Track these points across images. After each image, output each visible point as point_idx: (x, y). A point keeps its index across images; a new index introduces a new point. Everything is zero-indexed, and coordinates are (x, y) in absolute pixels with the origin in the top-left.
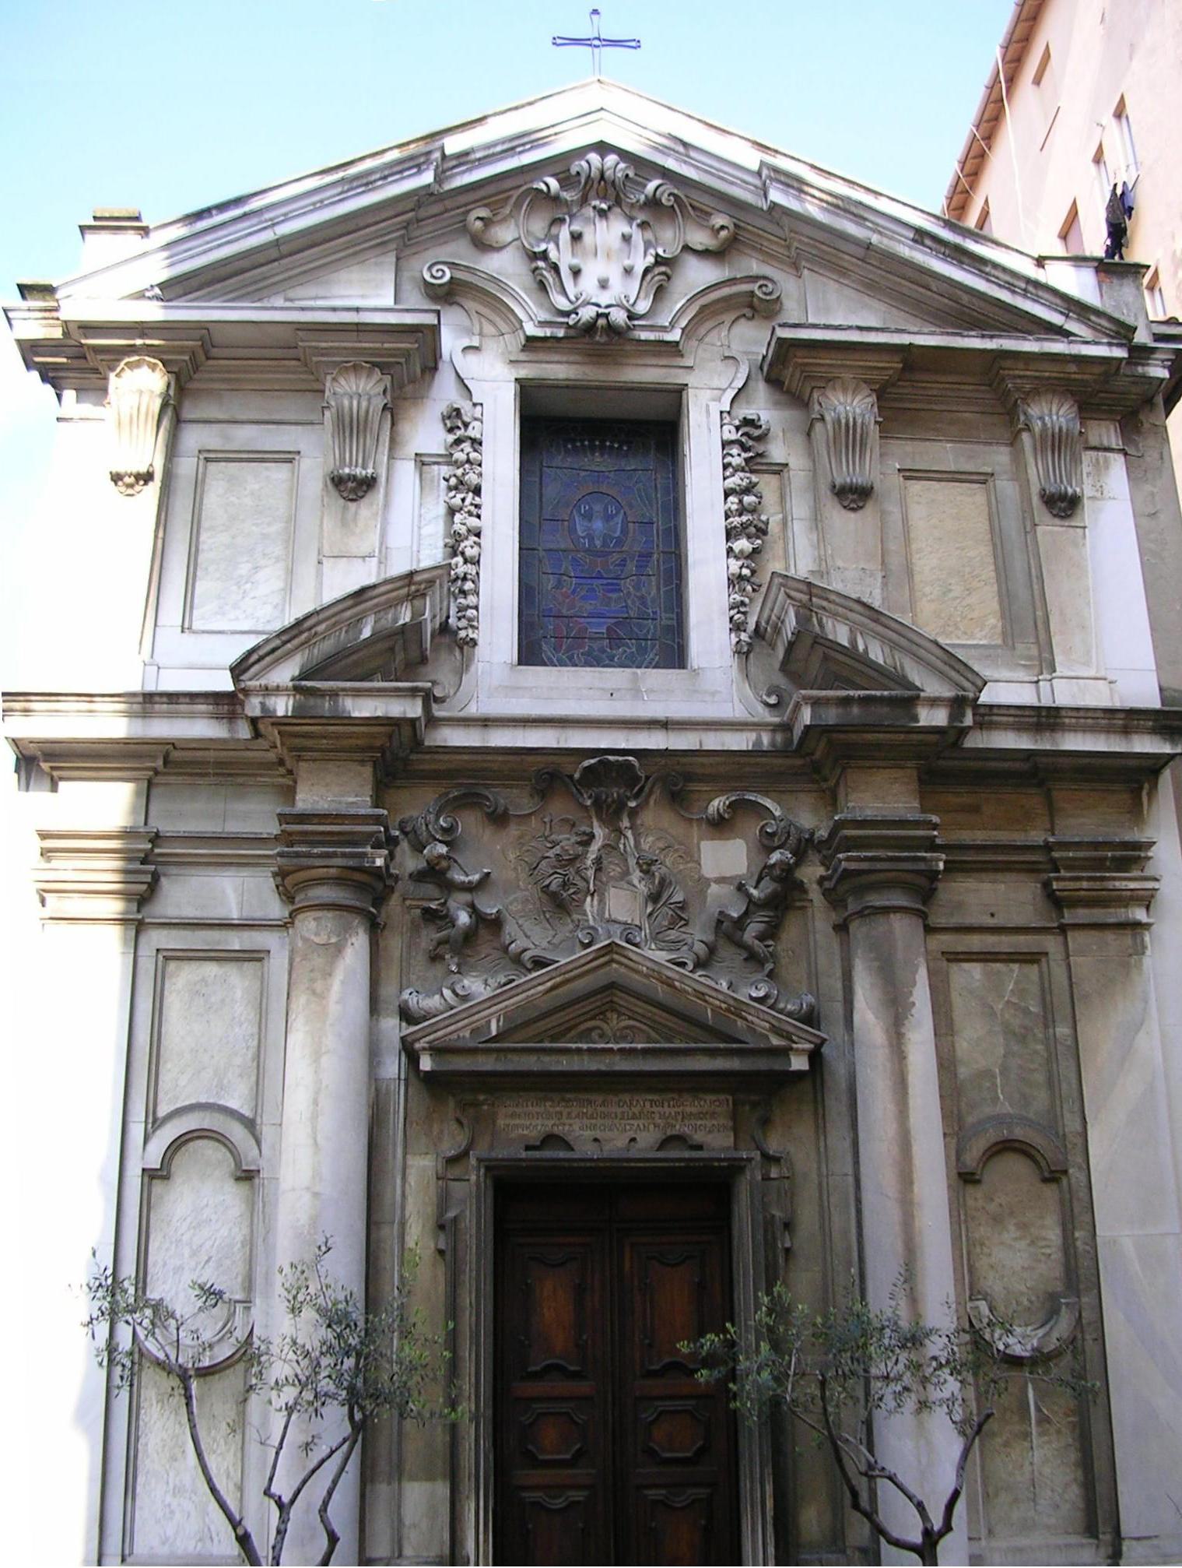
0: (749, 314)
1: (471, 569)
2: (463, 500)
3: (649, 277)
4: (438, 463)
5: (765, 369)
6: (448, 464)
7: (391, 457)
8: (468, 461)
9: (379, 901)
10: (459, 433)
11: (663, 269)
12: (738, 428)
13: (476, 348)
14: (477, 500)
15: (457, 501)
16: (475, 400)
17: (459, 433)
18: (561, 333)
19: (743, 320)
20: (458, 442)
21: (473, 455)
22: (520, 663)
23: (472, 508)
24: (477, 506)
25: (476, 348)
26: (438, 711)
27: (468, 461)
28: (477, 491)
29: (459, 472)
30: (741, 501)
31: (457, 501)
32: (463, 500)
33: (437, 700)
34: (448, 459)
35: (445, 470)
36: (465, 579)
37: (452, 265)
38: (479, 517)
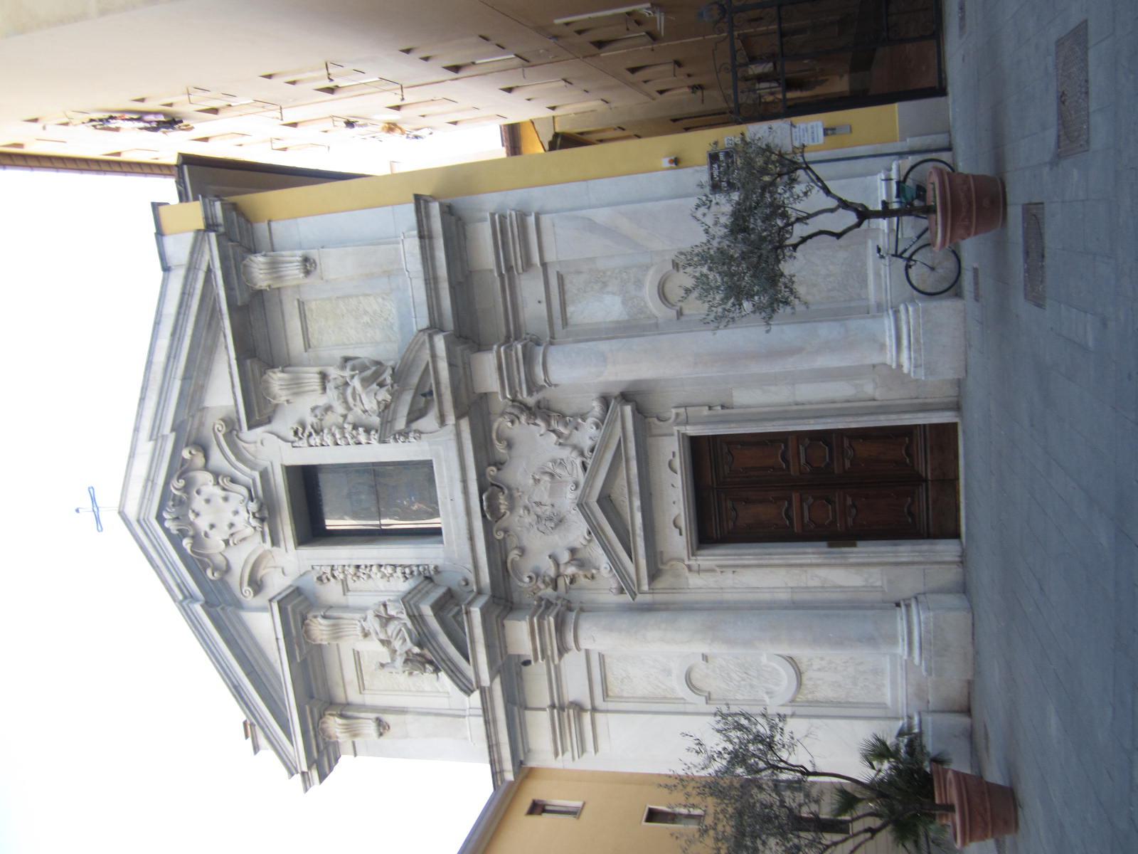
20: (334, 577)
23: (368, 569)
28: (358, 567)
36: (404, 573)
38: (371, 566)
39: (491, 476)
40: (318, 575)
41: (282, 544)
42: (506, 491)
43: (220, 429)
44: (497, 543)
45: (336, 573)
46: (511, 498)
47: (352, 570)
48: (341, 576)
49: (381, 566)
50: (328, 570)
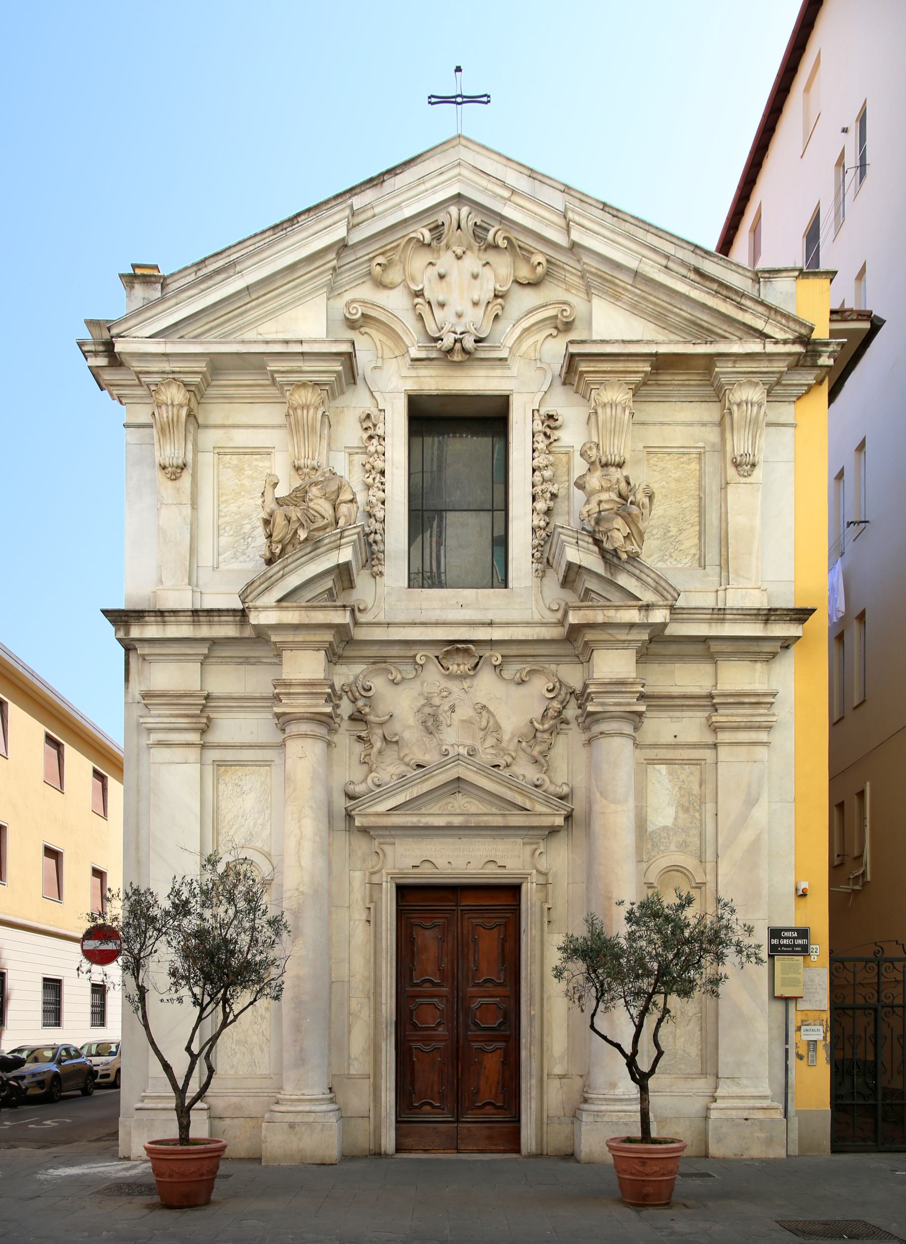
0: (555, 332)
1: (378, 526)
2: (374, 479)
3: (490, 306)
4: (357, 453)
5: (563, 375)
6: (365, 453)
7: (330, 449)
8: (376, 452)
9: (332, 730)
10: (371, 432)
11: (499, 301)
12: (543, 423)
13: (380, 368)
14: (383, 480)
15: (370, 480)
17: (371, 432)
18: (434, 355)
19: (550, 338)
20: (371, 437)
21: (380, 448)
22: (409, 587)
23: (380, 485)
24: (382, 483)
25: (380, 368)
26: (362, 618)
27: (376, 452)
28: (382, 473)
29: (371, 460)
30: (542, 476)
31: (370, 480)
32: (374, 479)
33: (360, 610)
34: (364, 450)
35: (362, 458)
36: (376, 533)
37: (364, 302)
38: (384, 491)
39: (491, 656)
41: (413, 373)
42: (472, 673)
43: (565, 314)
44: (412, 653)
45: (375, 441)
46: (463, 677)
47: (379, 464)
48: (372, 449)
49: (383, 503)
50: (380, 432)
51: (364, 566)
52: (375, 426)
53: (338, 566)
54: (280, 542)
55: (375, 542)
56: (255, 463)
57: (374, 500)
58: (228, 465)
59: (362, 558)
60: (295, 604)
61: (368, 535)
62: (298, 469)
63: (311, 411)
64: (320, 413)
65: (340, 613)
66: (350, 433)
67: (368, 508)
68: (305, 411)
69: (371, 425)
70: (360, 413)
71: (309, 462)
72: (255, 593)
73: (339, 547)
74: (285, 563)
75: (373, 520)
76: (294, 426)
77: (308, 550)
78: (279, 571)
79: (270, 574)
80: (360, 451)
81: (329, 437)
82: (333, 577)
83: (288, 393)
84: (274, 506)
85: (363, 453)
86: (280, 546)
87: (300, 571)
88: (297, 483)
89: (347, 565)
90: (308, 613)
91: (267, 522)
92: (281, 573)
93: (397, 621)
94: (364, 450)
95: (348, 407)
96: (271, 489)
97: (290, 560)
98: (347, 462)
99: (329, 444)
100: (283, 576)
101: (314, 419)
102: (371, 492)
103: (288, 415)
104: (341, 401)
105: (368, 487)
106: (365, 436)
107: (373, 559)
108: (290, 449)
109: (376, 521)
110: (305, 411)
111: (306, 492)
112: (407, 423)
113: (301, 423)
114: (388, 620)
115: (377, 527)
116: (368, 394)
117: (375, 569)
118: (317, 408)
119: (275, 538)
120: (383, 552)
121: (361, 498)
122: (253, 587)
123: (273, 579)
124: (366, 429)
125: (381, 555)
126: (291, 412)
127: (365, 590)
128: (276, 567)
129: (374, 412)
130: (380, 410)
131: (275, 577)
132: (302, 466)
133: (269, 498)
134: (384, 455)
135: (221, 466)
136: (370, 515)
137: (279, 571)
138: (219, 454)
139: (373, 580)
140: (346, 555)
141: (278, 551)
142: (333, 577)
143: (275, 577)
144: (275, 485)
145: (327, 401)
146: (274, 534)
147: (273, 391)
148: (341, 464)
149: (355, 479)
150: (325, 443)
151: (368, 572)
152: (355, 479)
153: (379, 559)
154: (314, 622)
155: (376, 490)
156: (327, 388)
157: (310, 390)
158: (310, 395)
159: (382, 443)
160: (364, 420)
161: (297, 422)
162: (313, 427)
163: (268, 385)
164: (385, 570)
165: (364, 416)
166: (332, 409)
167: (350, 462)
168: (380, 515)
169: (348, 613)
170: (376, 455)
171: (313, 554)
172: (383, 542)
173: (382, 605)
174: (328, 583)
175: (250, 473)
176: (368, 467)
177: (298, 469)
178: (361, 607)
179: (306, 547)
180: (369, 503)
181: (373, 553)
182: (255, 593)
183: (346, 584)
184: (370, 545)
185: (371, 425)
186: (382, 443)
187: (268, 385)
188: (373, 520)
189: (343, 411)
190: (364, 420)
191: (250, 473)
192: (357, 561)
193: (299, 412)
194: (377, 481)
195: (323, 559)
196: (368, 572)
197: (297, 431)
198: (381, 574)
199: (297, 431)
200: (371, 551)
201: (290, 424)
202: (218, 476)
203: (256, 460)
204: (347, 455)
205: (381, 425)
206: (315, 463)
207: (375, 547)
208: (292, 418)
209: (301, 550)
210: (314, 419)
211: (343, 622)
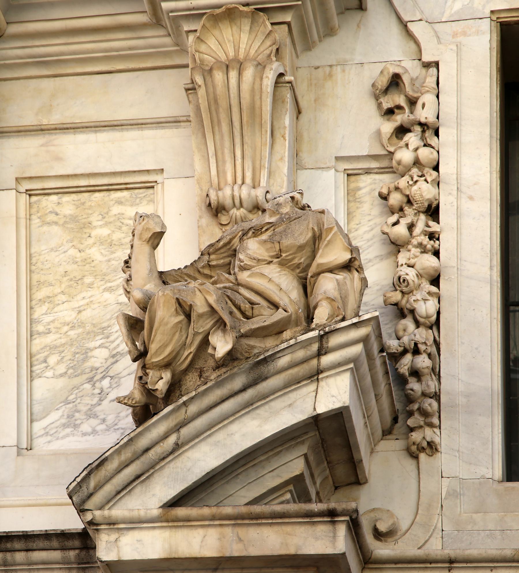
1: (423, 335)
2: (411, 227)
4: (368, 172)
6: (390, 170)
8: (417, 163)
10: (399, 119)
14: (434, 227)
15: (401, 230)
16: (427, 58)
17: (399, 119)
20: (402, 131)
21: (425, 154)
23: (425, 240)
24: (433, 236)
26: (382, 550)
27: (417, 163)
28: (433, 212)
29: (403, 182)
31: (401, 230)
32: (411, 227)
35: (383, 182)
36: (416, 351)
38: (437, 253)
40: (405, 79)
45: (413, 139)
47: (424, 191)
48: (405, 156)
49: (435, 281)
50: (425, 113)
51: (387, 433)
52: (412, 102)
53: (316, 420)
54: (167, 365)
55: (416, 373)
56: (116, 210)
57: (411, 275)
58: (52, 218)
59: (381, 408)
60: (206, 511)
61: (396, 357)
62: (216, 210)
63: (249, 73)
64: (270, 77)
65: (323, 529)
66: (351, 122)
67: (396, 296)
68: (233, 74)
69: (401, 101)
70: (374, 74)
71: (245, 192)
72: (109, 488)
73: (315, 375)
74: (181, 416)
75: (408, 323)
76: (209, 115)
77: (238, 383)
78: (166, 436)
79: (143, 442)
80: (374, 165)
81: (297, 139)
82: (304, 449)
83: (191, 38)
84: (152, 286)
85: (382, 171)
86: (167, 376)
87: (220, 436)
88: (214, 234)
89: (339, 417)
90: (242, 532)
91: (134, 325)
92: (172, 439)
93: (474, 552)
94: (385, 163)
95: (343, 64)
96: (147, 248)
97: (193, 409)
98: (342, 193)
99: (296, 155)
100: (177, 446)
101: (256, 91)
102: (402, 258)
103: (191, 89)
104: (326, 52)
105: (396, 246)
106: (388, 127)
107: (410, 414)
108: (199, 166)
109: (418, 324)
110: (233, 74)
111: (234, 254)
112: (496, 90)
113: (223, 103)
114: (450, 552)
115: (418, 338)
116: (395, 29)
117: (416, 436)
118: (261, 67)
119: (155, 357)
120: (437, 396)
121: (377, 273)
122: (103, 473)
123: (152, 454)
124: (390, 112)
125: (430, 405)
126: (199, 80)
127: (390, 486)
128: (158, 426)
129: (411, 70)
130: (427, 65)
131: (158, 450)
132: (228, 202)
133: (140, 268)
134: (436, 168)
135: (36, 221)
136: (401, 312)
137: (166, 436)
138: (30, 193)
139: (410, 464)
140: (335, 393)
141: (161, 386)
142: (304, 449)
143: (158, 450)
144: (156, 238)
145: (287, 51)
146: (153, 347)
147: (156, 38)
148: (325, 192)
149: (364, 227)
150: (284, 148)
151: (400, 444)
152: (364, 227)
153: (425, 414)
154: (254, 552)
155: (415, 251)
156: (288, 17)
157: (246, 24)
158: (245, 37)
159: (433, 141)
160: (386, 91)
161: (213, 102)
162: (254, 111)
163: (143, 26)
164: (444, 438)
165: (384, 82)
166: (303, 73)
167: (351, 194)
168: (426, 308)
169: (342, 530)
170: (415, 171)
171: (250, 393)
172: (436, 372)
173: (436, 520)
174: (292, 464)
175: (105, 232)
176: (395, 199)
177: (216, 210)
178: (382, 527)
179: (232, 377)
180: (399, 283)
181: (409, 400)
182: (109, 488)
183: (342, 471)
184: (402, 381)
185: (401, 101)
186: (433, 141)
187: (143, 26)
188: (408, 323)
189: (330, 75)
190: (386, 91)
191: (105, 232)
192: (367, 416)
193: (219, 76)
194: (417, 230)
195: (277, 404)
196: (400, 444)
197: (215, 123)
198: (432, 448)
199: (215, 123)
200: (404, 392)
201: (198, 109)
202: (29, 245)
203: (119, 202)
204: (342, 177)
205: (428, 98)
206: (259, 193)
207: (414, 385)
208: (201, 92)
209: (219, 384)
210: (256, 91)
211: (329, 551)
